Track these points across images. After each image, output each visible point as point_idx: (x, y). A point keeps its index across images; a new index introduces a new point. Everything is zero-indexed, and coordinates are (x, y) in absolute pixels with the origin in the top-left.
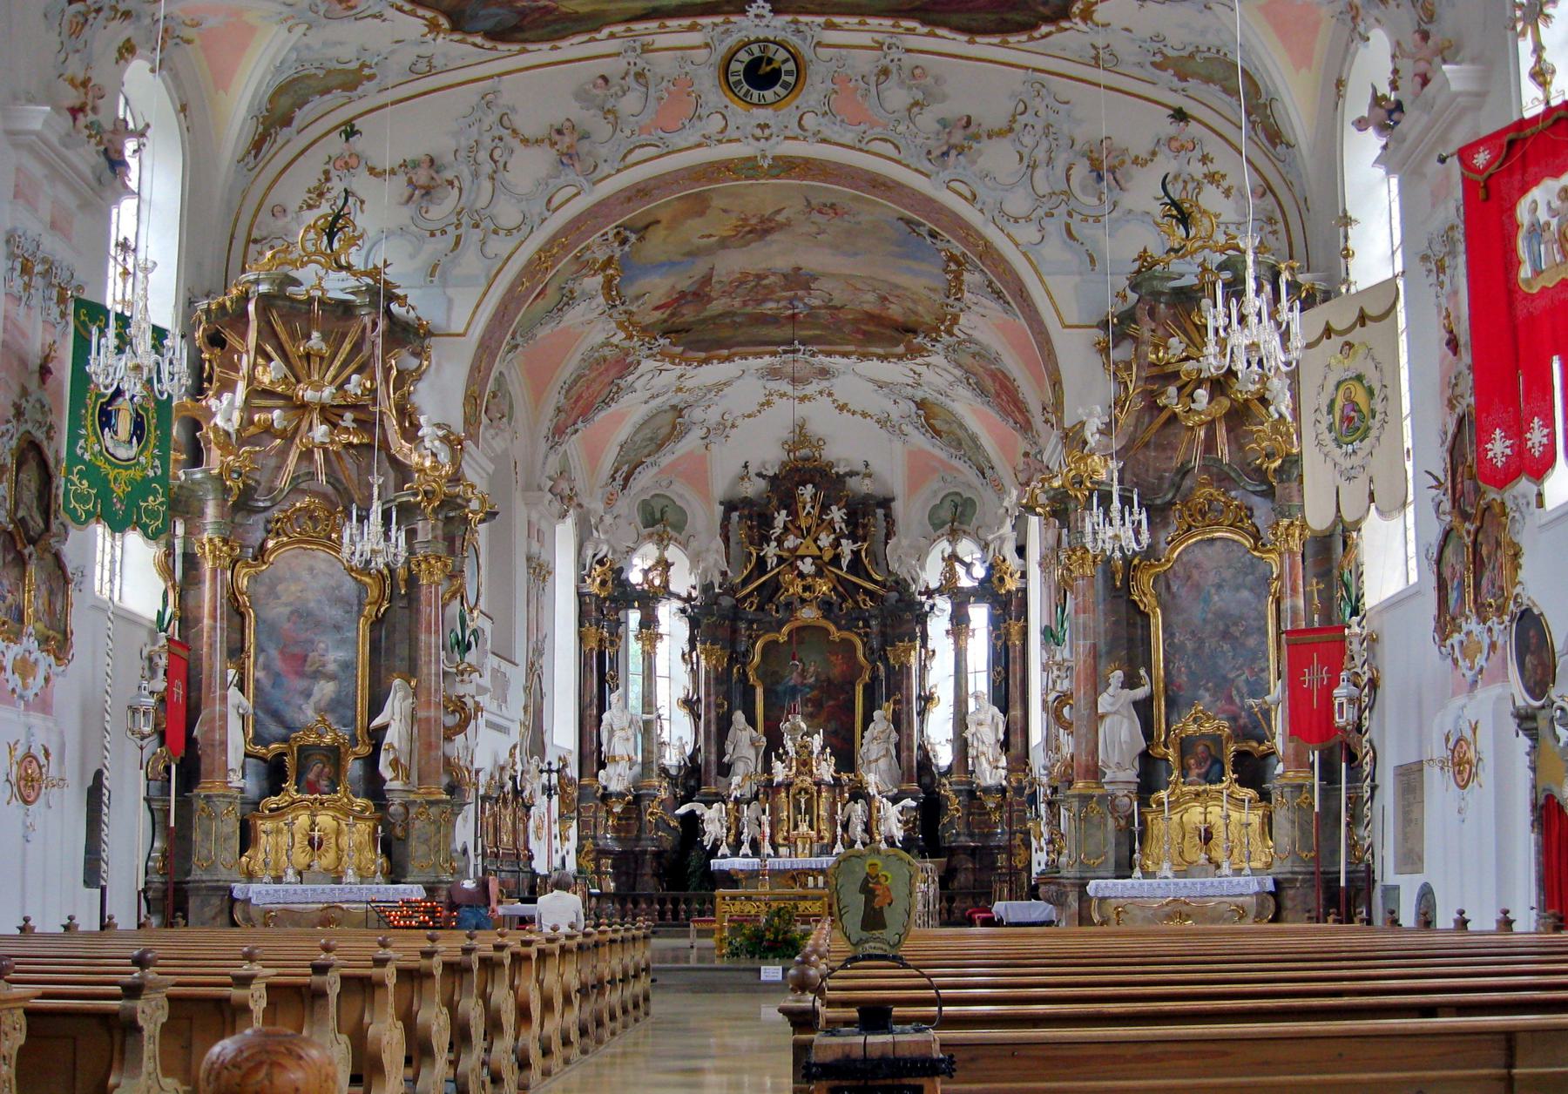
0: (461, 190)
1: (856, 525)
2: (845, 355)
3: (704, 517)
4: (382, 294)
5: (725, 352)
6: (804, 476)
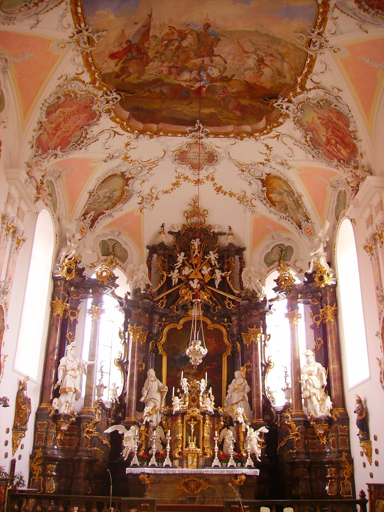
1: (223, 264)
2: (227, 135)
5: (154, 127)
6: (195, 240)
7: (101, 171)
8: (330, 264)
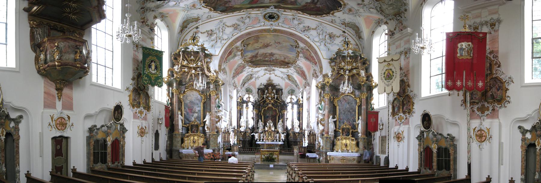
3: (255, 91)
7: (246, 75)
8: (302, 97)
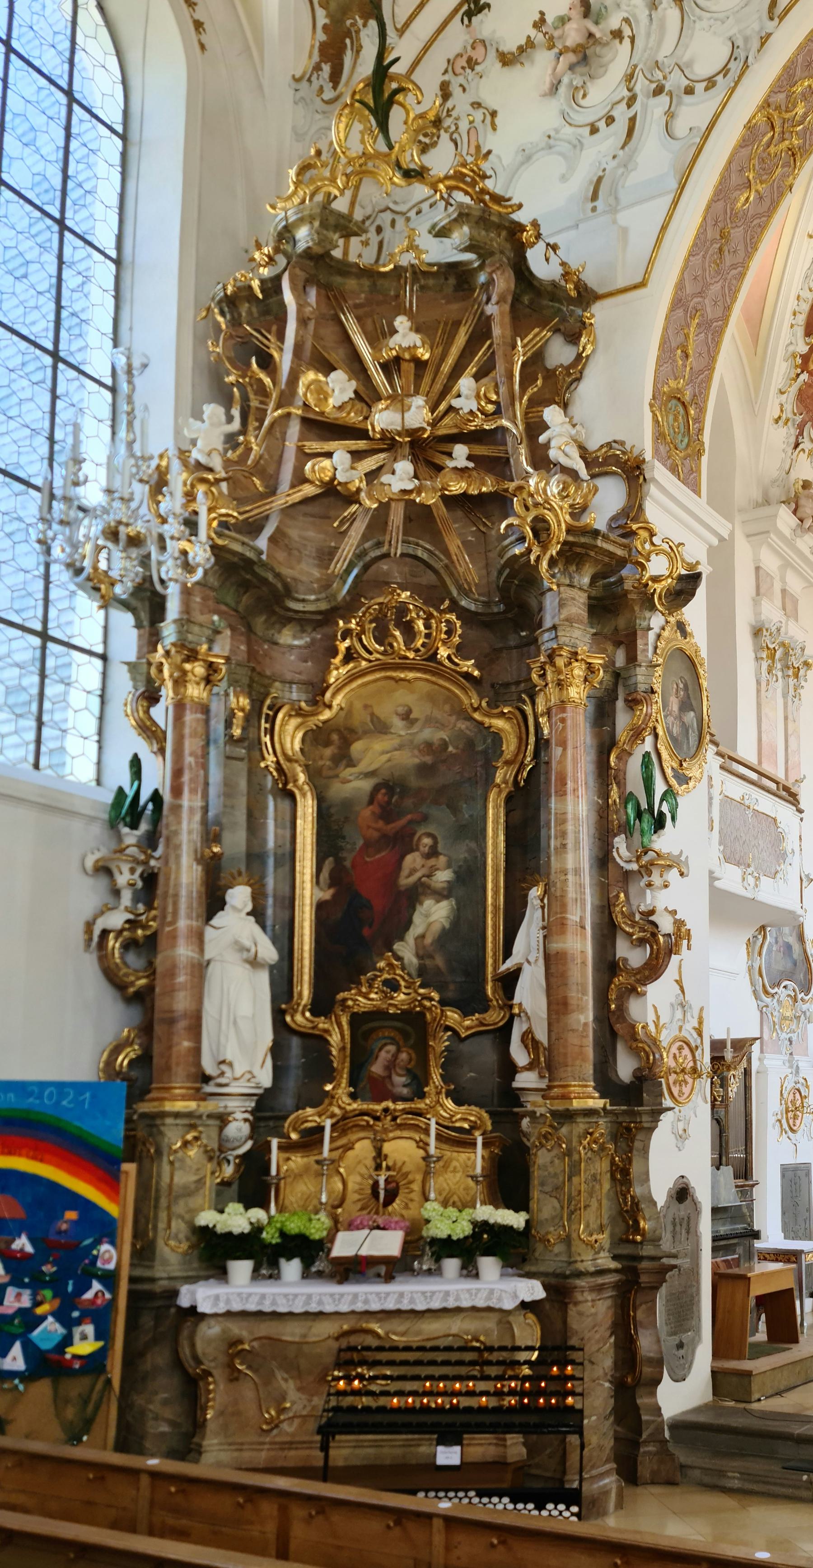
0: (633, 39)
4: (501, 233)
